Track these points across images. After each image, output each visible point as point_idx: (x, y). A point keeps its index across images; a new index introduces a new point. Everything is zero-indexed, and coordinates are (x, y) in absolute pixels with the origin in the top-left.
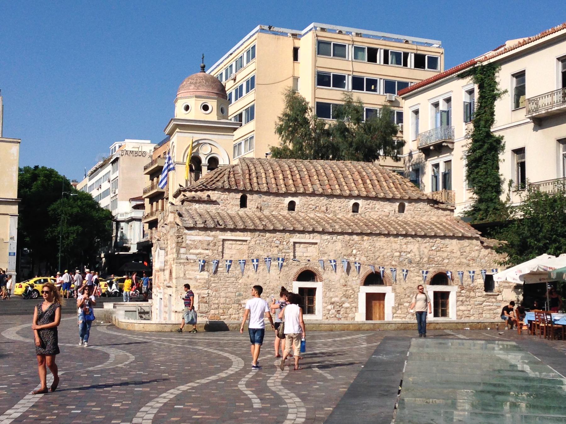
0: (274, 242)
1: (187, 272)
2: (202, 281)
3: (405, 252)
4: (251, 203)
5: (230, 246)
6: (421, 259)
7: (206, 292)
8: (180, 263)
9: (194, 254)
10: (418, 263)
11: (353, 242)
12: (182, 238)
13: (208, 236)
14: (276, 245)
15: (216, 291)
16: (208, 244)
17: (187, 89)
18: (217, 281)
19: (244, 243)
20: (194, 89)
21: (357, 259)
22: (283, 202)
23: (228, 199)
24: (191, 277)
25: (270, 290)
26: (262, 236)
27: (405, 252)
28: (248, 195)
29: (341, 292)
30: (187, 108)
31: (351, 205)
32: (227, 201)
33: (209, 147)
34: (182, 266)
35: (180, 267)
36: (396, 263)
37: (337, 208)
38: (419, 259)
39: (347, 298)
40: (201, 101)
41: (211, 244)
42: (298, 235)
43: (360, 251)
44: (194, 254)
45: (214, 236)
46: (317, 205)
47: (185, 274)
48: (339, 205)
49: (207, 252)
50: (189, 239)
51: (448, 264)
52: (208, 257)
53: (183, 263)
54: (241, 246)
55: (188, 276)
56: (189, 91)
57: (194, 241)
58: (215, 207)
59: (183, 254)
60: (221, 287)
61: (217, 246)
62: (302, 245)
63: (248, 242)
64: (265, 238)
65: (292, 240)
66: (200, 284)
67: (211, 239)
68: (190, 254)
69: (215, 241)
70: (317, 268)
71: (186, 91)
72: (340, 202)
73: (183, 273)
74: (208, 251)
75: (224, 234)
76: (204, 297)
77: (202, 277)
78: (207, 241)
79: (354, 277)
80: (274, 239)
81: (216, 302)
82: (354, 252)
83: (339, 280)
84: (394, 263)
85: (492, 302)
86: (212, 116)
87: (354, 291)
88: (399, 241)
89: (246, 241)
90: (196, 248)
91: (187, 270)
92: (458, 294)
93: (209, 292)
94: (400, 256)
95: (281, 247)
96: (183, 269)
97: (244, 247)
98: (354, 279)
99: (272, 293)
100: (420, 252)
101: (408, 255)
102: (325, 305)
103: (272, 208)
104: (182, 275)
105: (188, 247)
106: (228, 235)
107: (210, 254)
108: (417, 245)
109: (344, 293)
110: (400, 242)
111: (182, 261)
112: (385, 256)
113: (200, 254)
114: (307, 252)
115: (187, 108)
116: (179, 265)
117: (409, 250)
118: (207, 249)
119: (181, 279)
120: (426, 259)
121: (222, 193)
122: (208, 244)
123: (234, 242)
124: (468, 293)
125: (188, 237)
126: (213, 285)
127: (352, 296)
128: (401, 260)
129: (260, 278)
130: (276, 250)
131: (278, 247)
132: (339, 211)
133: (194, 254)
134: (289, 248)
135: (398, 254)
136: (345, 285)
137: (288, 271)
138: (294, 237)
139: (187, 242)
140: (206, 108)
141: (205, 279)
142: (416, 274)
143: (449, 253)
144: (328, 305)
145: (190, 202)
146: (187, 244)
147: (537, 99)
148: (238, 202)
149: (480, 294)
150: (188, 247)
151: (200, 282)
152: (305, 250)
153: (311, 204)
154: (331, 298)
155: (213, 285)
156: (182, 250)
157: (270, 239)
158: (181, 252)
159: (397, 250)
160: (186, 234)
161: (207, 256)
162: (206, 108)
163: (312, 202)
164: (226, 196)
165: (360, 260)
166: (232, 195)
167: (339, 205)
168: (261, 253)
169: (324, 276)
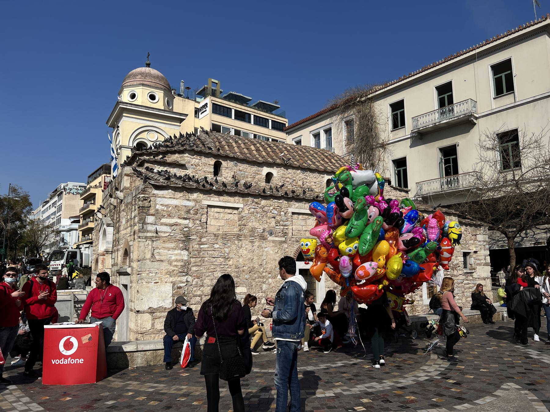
0: (271, 212)
1: (156, 251)
2: (179, 264)
4: (227, 171)
5: (217, 215)
7: (184, 279)
8: (146, 238)
12: (150, 202)
13: (188, 200)
14: (272, 215)
15: (198, 278)
16: (188, 212)
17: (134, 79)
18: (199, 264)
19: (235, 212)
20: (140, 78)
22: (261, 173)
23: (200, 164)
25: (267, 274)
26: (256, 203)
28: (223, 162)
30: (133, 96)
31: (325, 181)
32: (199, 167)
33: (156, 134)
34: (150, 243)
35: (146, 243)
37: (313, 183)
40: (148, 91)
41: (191, 212)
42: (297, 204)
45: (195, 200)
46: (295, 179)
47: (153, 254)
48: (315, 180)
49: (187, 222)
50: (161, 203)
52: (187, 229)
53: (151, 238)
54: (230, 215)
55: (157, 257)
56: (136, 80)
57: (167, 206)
58: (184, 173)
59: (151, 224)
60: (204, 271)
61: (199, 215)
62: (301, 217)
63: (240, 210)
64: (260, 206)
65: (291, 210)
66: (176, 269)
67: (191, 204)
68: (162, 224)
69: (197, 207)
71: (133, 80)
72: (315, 178)
73: (150, 252)
74: (188, 221)
75: (209, 198)
76: (180, 288)
77: (179, 258)
78: (185, 206)
80: (271, 208)
81: (199, 293)
85: (470, 280)
86: (160, 104)
89: (237, 209)
90: (169, 216)
91: (157, 248)
93: (189, 280)
95: (278, 218)
96: (150, 247)
97: (234, 217)
99: (269, 278)
103: (250, 179)
104: (148, 256)
105: (158, 214)
106: (215, 200)
111: (149, 234)
113: (176, 224)
114: (307, 225)
115: (133, 96)
118: (185, 219)
119: (148, 261)
121: (192, 157)
122: (188, 212)
123: (222, 210)
126: (194, 269)
129: (255, 258)
130: (273, 222)
131: (274, 218)
132: (315, 187)
133: (166, 225)
134: (287, 220)
137: (287, 248)
138: (293, 206)
140: (152, 97)
141: (182, 260)
145: (152, 164)
146: (157, 210)
147: (418, 118)
148: (212, 170)
149: (460, 272)
150: (158, 214)
151: (176, 266)
152: (303, 223)
153: (289, 178)
155: (194, 269)
156: (150, 219)
157: (266, 208)
158: (148, 222)
160: (155, 196)
161: (186, 228)
162: (152, 97)
163: (289, 176)
164: (197, 160)
166: (204, 159)
167: (315, 180)
168: (256, 224)
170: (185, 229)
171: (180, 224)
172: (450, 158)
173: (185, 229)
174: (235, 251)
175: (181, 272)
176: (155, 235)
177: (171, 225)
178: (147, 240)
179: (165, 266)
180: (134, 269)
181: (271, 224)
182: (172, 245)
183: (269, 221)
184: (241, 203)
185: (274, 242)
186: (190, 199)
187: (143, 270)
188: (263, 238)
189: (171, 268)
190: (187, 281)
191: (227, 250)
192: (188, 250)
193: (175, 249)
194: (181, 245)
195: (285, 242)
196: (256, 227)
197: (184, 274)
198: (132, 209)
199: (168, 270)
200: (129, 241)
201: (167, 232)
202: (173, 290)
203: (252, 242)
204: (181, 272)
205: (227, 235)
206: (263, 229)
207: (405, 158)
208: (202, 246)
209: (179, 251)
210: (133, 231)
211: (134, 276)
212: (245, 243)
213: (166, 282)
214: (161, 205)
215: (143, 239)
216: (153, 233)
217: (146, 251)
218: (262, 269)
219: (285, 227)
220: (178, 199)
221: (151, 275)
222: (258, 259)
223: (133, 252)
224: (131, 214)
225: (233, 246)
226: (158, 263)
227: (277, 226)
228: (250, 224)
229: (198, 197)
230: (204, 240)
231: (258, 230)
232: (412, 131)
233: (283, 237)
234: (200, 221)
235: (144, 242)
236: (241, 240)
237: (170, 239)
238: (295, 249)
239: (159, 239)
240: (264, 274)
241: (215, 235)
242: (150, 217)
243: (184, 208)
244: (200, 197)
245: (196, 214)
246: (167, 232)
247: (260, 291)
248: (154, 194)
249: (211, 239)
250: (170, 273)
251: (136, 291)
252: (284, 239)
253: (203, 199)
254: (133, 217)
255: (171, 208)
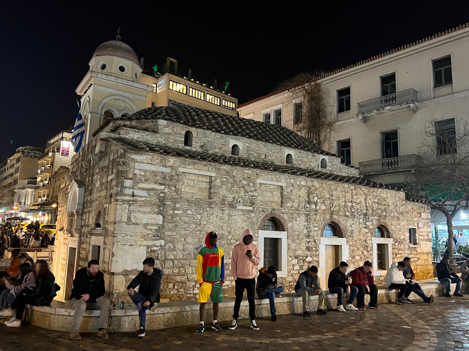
3: (355, 203)
6: (367, 210)
7: (158, 243)
8: (123, 201)
9: (143, 189)
10: (365, 215)
11: (313, 188)
13: (165, 166)
16: (165, 178)
21: (318, 208)
24: (138, 222)
25: (235, 241)
27: (355, 203)
29: (304, 245)
34: (127, 206)
35: (123, 206)
36: (349, 214)
38: (366, 211)
39: (309, 251)
43: (320, 198)
44: (143, 189)
47: (129, 218)
51: (385, 216)
52: (163, 195)
55: (133, 221)
57: (145, 171)
59: (129, 188)
66: (151, 232)
68: (139, 188)
69: (174, 173)
70: (282, 215)
73: (126, 215)
74: (163, 187)
76: (154, 251)
77: (154, 222)
78: (162, 172)
79: (315, 227)
82: (316, 199)
83: (303, 229)
84: (347, 213)
87: (315, 243)
88: (351, 191)
90: (146, 180)
92: (393, 247)
94: (352, 207)
96: (127, 210)
98: (316, 229)
100: (366, 203)
101: (358, 206)
102: (290, 259)
104: (125, 219)
107: (166, 191)
108: (364, 197)
109: (307, 245)
110: (352, 192)
111: (126, 198)
112: (341, 206)
113: (153, 189)
116: (121, 203)
117: (358, 201)
118: (161, 184)
119: (124, 224)
120: (371, 211)
124: (399, 245)
125: (137, 165)
127: (314, 249)
128: (352, 211)
131: (243, 187)
135: (350, 204)
136: (309, 236)
137: (254, 217)
139: (136, 172)
142: (364, 225)
143: (386, 206)
144: (292, 259)
154: (295, 250)
156: (128, 183)
158: (126, 186)
159: (350, 200)
165: (320, 208)
168: (227, 194)
169: (290, 225)
170: (161, 195)
171: (156, 190)
172: (391, 142)
173: (161, 195)
174: (206, 218)
175: (154, 236)
176: (132, 198)
177: (148, 190)
178: (124, 204)
179: (140, 229)
180: (109, 232)
181: (241, 194)
182: (148, 209)
183: (238, 191)
184: (213, 172)
185: (242, 210)
186: (166, 165)
187: (119, 232)
188: (232, 206)
189: (146, 231)
190: (161, 246)
191: (199, 217)
192: (162, 215)
193: (150, 213)
194: (157, 210)
195: (252, 211)
196: (227, 195)
197: (158, 238)
198: (108, 172)
199: (143, 233)
200: (104, 203)
201: (143, 197)
202: (147, 254)
203: (222, 210)
204: (154, 236)
205: (200, 202)
206: (233, 198)
207: (350, 139)
208: (176, 212)
209: (155, 215)
210: (108, 194)
211: (108, 238)
212: (217, 212)
213: (140, 245)
214: (140, 169)
215: (120, 202)
216: (130, 197)
217: (123, 214)
218: (230, 237)
219: (253, 197)
220: (155, 165)
221: (126, 237)
222: (227, 226)
223: (108, 215)
224: (107, 177)
225: (205, 213)
226: (134, 226)
227: (246, 195)
228: (221, 193)
229: (174, 164)
230: (177, 205)
231: (228, 198)
232: (357, 115)
233: (251, 206)
234: (175, 187)
235: (121, 205)
236: (212, 208)
237: (145, 203)
238: (262, 218)
239: (135, 203)
240: (232, 241)
241: (188, 201)
242: (128, 180)
243: (161, 174)
244: (176, 164)
245: (171, 180)
246: (143, 197)
247: (228, 258)
248: (133, 159)
249: (186, 206)
250: (144, 237)
251: (111, 253)
252: (251, 208)
253: (178, 166)
254: (109, 180)
255: (148, 173)
